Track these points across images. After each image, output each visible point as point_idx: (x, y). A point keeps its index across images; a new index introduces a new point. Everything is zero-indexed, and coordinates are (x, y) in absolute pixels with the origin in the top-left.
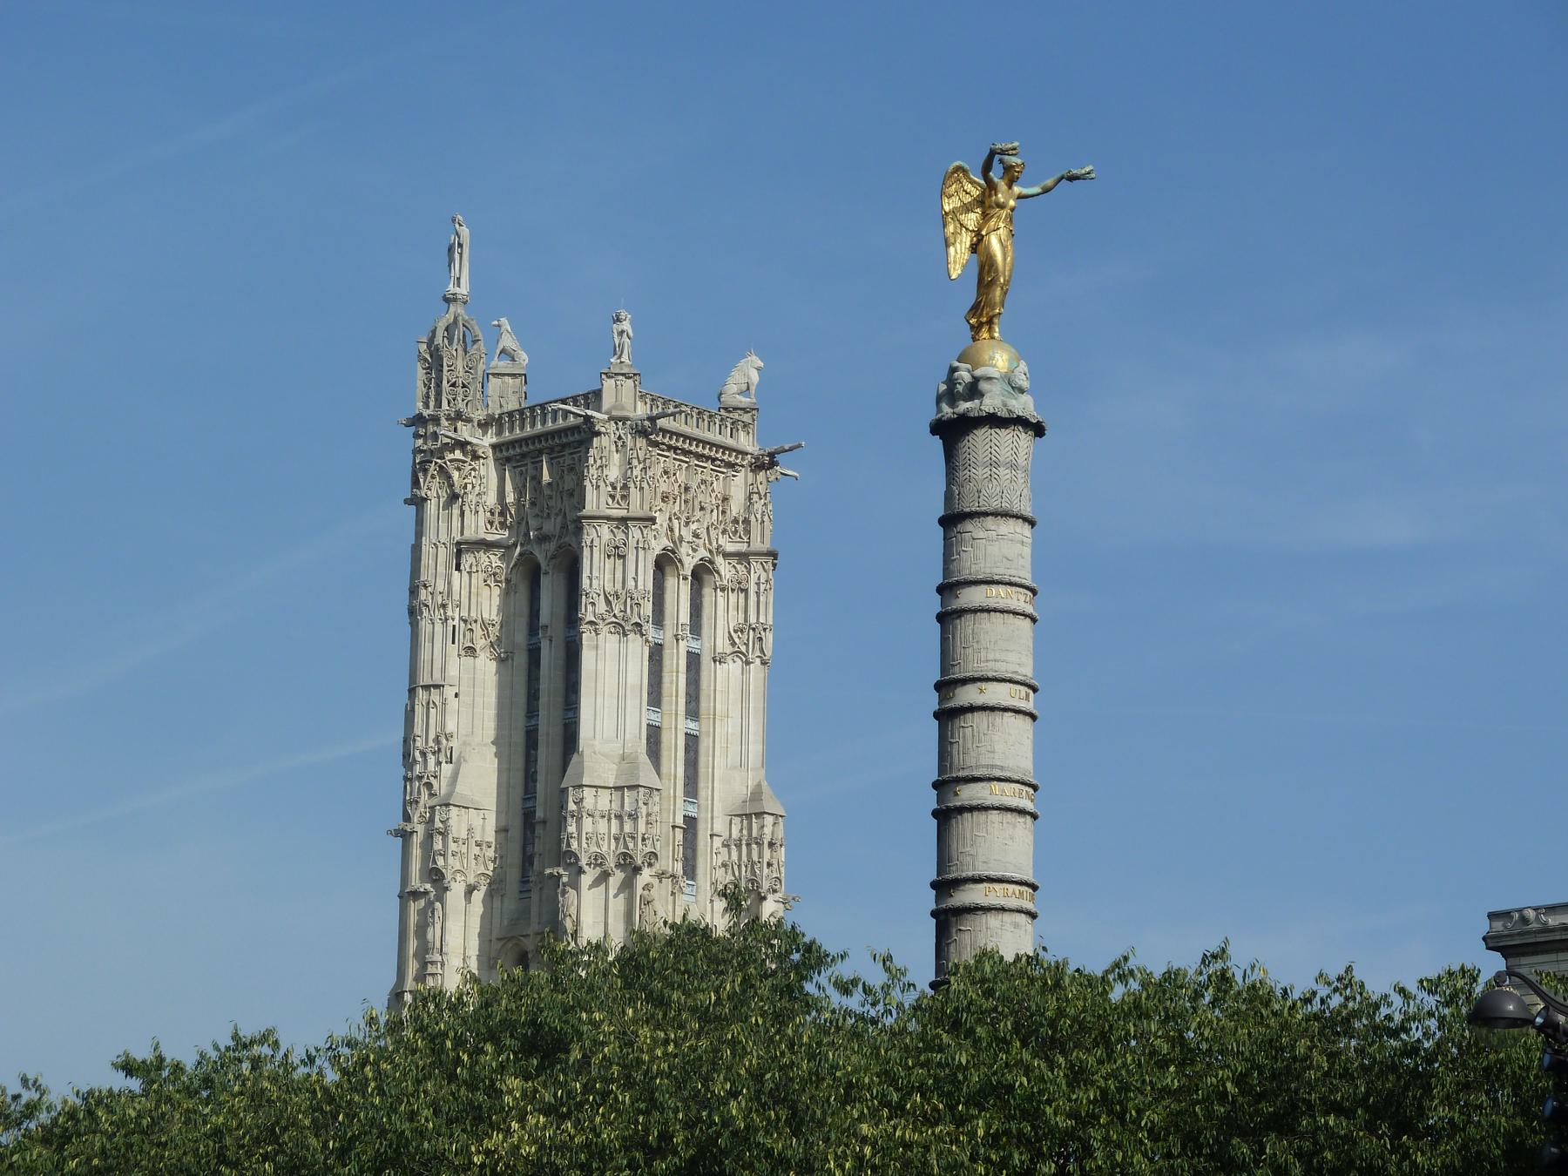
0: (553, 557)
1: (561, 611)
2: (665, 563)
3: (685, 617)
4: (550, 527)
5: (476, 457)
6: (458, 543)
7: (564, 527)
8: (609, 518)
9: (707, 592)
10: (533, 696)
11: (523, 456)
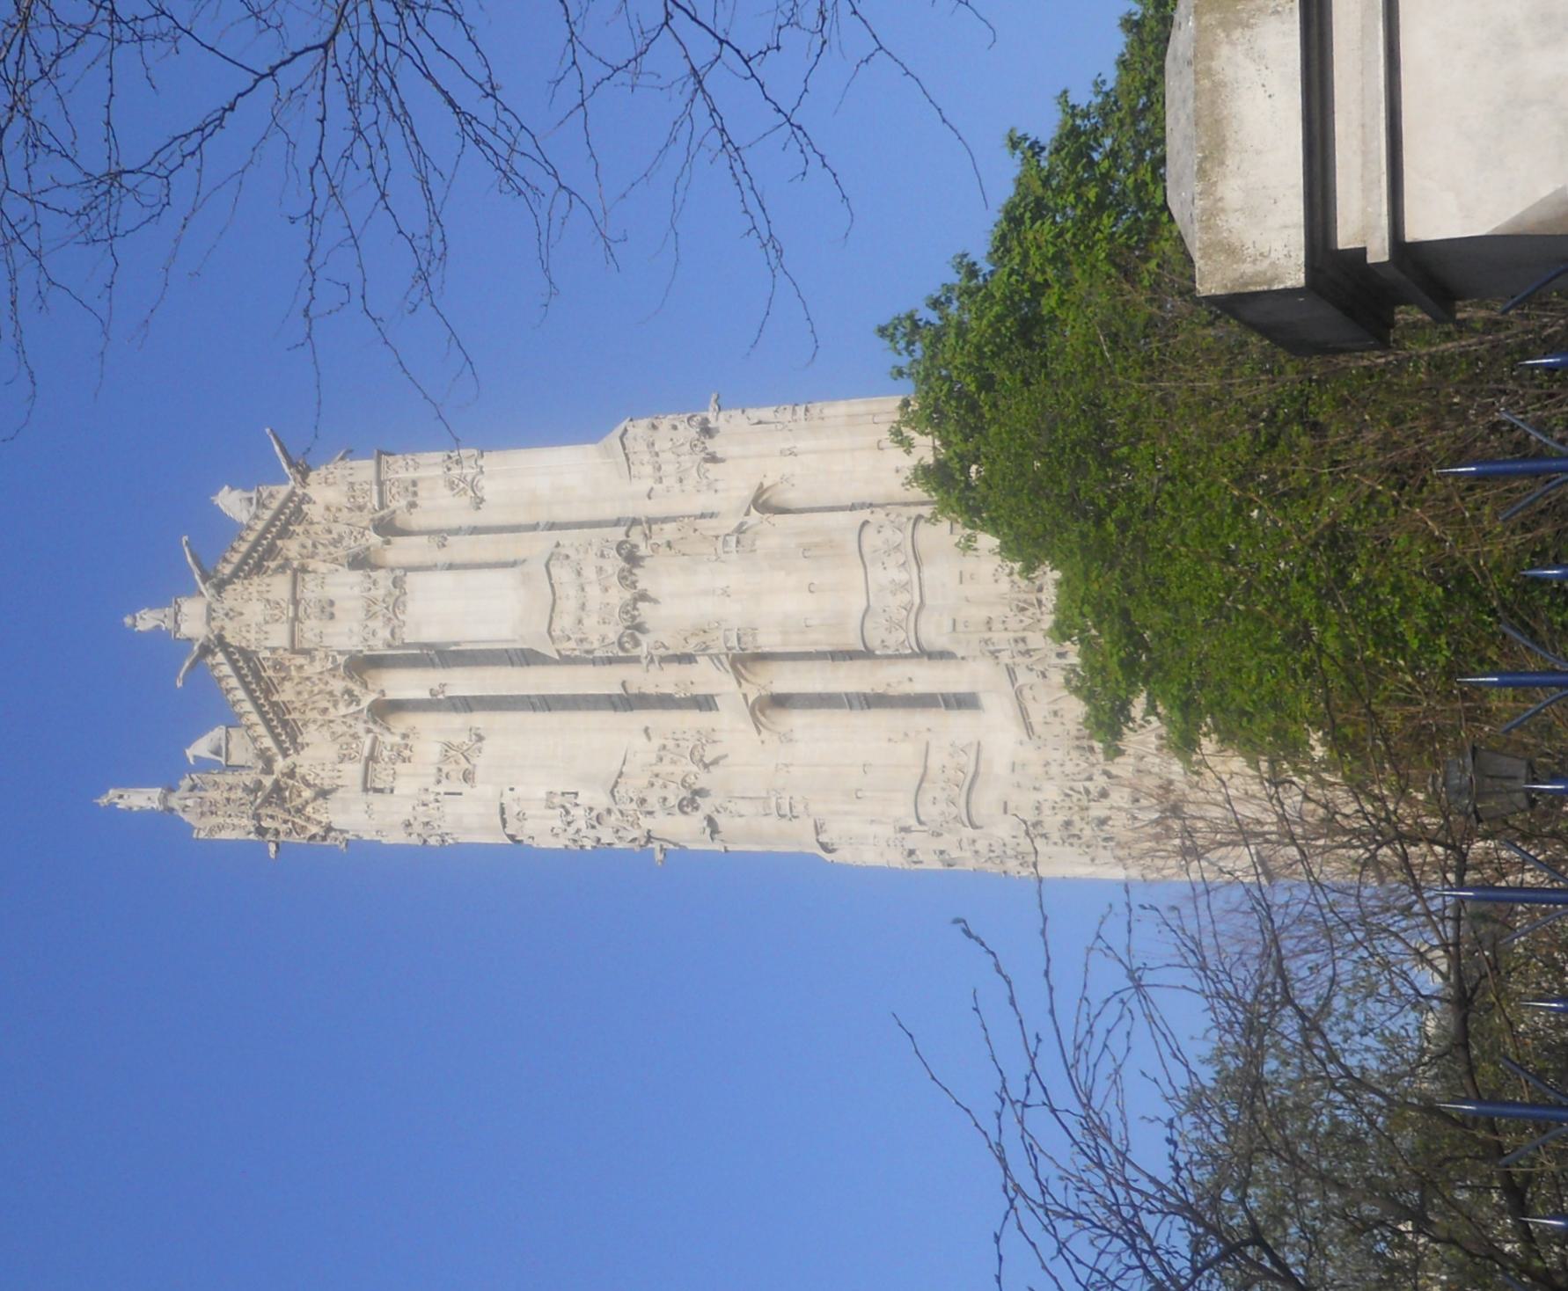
5: (291, 774)
6: (366, 790)
8: (296, 618)
11: (285, 724)
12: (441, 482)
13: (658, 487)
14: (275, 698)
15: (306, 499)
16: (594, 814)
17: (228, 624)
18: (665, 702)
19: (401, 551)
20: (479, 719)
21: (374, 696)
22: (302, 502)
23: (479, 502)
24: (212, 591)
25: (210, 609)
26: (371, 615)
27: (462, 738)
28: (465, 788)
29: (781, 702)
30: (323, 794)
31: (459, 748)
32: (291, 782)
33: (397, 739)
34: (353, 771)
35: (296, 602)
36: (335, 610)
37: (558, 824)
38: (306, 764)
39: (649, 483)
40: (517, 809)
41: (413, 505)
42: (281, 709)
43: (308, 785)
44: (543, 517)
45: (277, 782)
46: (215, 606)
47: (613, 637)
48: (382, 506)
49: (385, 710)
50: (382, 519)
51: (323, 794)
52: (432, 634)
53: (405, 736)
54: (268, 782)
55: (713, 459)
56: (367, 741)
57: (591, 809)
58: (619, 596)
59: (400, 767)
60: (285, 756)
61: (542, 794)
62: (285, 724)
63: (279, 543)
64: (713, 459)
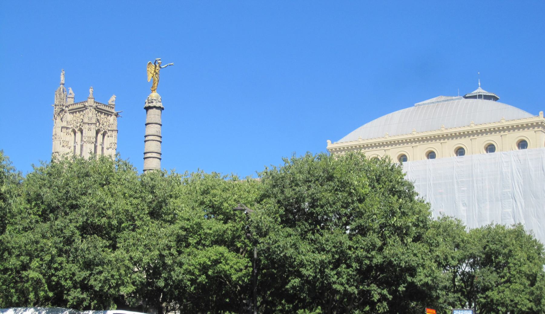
5: (65, 112)
9: (106, 137)
15: (111, 115)
19: (100, 136)
23: (108, 149)
25: (92, 106)
26: (88, 137)
30: (61, 119)
34: (64, 124)
35: (91, 124)
42: (76, 112)
48: (109, 130)
51: (61, 119)
54: (64, 108)
56: (70, 127)
60: (69, 110)
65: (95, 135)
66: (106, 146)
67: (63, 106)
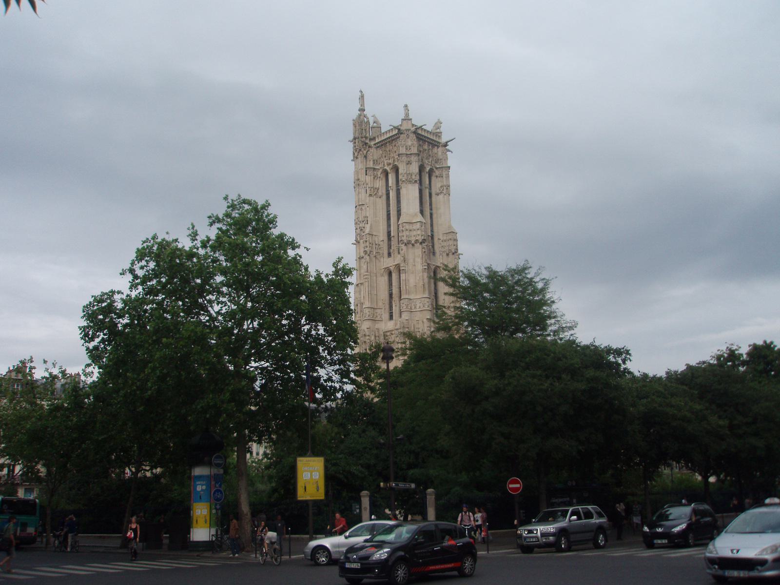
0: (392, 169)
1: (395, 182)
2: (421, 168)
3: (427, 182)
4: (391, 161)
5: (369, 147)
7: (394, 161)
8: (407, 154)
9: (433, 178)
10: (388, 205)
11: (382, 145)
12: (442, 184)
13: (441, 241)
14: (388, 144)
15: (438, 147)
16: (363, 228)
17: (405, 135)
18: (390, 247)
20: (384, 197)
21: (389, 171)
22: (437, 146)
23: (437, 194)
24: (414, 130)
25: (409, 130)
27: (380, 194)
28: (368, 195)
29: (390, 274)
30: (365, 157)
31: (377, 192)
32: (367, 147)
33: (379, 176)
34: (371, 164)
36: (409, 165)
37: (360, 219)
38: (372, 151)
39: (442, 239)
40: (363, 208)
41: (437, 177)
43: (367, 152)
44: (434, 211)
45: (367, 143)
46: (410, 132)
47: (403, 239)
48: (437, 168)
49: (386, 174)
50: (433, 169)
51: (365, 157)
52: (403, 192)
53: (380, 177)
54: (367, 141)
55: (448, 255)
56: (378, 167)
57: (364, 228)
58: (413, 240)
59: (372, 177)
60: (375, 144)
61: (367, 215)
62: (382, 145)
63: (427, 143)
64: (448, 255)
65: (417, 170)
66: (434, 190)
67: (366, 138)
